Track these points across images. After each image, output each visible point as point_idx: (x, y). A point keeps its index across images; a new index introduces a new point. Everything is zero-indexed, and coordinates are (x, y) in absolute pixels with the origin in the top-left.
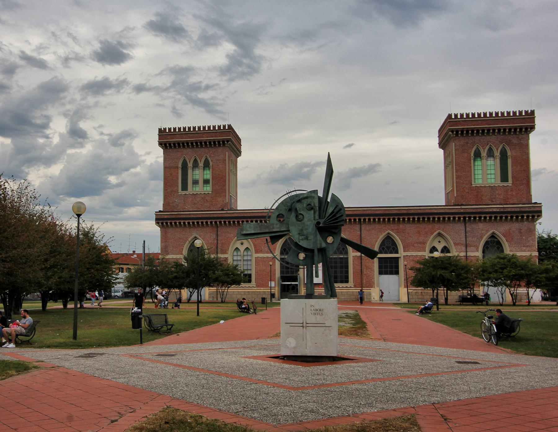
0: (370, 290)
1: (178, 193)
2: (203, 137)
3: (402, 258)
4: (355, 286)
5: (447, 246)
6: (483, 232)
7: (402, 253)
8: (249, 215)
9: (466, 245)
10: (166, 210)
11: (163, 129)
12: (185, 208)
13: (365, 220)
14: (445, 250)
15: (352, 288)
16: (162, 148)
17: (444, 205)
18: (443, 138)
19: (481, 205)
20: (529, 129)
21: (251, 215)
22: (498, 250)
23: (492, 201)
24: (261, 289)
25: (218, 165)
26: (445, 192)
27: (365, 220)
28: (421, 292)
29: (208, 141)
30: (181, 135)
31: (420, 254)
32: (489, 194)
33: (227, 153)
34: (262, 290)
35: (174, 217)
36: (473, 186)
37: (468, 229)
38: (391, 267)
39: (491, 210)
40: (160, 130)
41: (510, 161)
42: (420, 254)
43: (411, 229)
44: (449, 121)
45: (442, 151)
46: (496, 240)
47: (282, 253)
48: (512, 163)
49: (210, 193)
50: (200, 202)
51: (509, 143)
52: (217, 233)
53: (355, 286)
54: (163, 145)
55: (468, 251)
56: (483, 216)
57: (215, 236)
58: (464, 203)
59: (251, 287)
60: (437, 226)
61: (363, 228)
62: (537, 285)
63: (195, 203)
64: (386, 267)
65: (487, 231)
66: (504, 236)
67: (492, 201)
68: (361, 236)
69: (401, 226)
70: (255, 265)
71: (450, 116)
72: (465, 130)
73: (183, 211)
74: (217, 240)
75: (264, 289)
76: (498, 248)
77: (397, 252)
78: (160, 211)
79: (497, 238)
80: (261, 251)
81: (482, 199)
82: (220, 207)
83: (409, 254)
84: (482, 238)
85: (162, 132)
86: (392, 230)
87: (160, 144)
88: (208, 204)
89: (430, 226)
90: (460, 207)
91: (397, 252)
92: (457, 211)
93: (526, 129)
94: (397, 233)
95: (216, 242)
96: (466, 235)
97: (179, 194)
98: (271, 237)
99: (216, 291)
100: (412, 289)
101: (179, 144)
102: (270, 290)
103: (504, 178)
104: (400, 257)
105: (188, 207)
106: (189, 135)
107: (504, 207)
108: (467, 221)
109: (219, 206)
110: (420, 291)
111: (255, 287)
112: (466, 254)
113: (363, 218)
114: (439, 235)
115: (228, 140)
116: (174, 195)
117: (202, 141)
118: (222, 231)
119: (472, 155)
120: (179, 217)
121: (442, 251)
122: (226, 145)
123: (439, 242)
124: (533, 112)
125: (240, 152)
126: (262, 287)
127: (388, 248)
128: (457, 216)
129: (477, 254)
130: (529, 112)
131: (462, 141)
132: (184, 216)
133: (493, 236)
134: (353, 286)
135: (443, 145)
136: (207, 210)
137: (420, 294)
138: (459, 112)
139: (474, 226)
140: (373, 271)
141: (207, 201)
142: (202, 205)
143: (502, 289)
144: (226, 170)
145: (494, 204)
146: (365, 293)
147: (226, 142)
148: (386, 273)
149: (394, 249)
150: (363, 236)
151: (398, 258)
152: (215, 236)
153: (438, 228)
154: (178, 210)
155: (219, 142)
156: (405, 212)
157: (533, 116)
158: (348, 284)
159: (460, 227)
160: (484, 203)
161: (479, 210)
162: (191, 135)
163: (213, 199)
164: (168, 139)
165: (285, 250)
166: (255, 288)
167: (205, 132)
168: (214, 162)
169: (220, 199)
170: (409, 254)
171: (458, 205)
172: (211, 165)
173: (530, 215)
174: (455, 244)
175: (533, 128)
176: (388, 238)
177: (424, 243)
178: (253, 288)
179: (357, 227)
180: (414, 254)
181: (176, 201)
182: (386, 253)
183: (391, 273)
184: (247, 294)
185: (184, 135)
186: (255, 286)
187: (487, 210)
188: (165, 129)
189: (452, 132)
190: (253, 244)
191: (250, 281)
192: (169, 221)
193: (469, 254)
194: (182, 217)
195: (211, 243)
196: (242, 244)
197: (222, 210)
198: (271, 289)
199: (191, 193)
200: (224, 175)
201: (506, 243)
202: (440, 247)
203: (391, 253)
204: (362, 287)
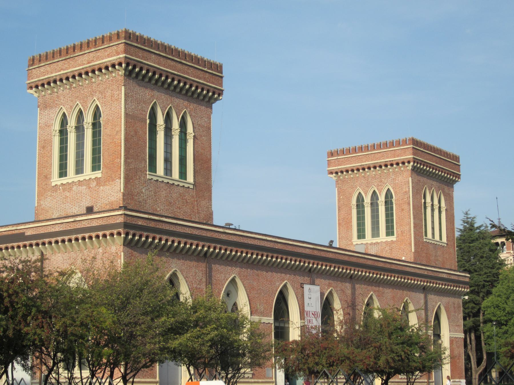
2: (188, 74)
12: (156, 210)
23: (436, 264)
35: (152, 225)
73: (166, 217)
97: (148, 177)
109: (202, 216)
115: (221, 92)
120: (160, 226)
141: (187, 202)
142: (180, 209)
162: (173, 63)
164: (139, 57)
169: (203, 203)
181: (144, 191)
185: (162, 59)
186: (251, 376)
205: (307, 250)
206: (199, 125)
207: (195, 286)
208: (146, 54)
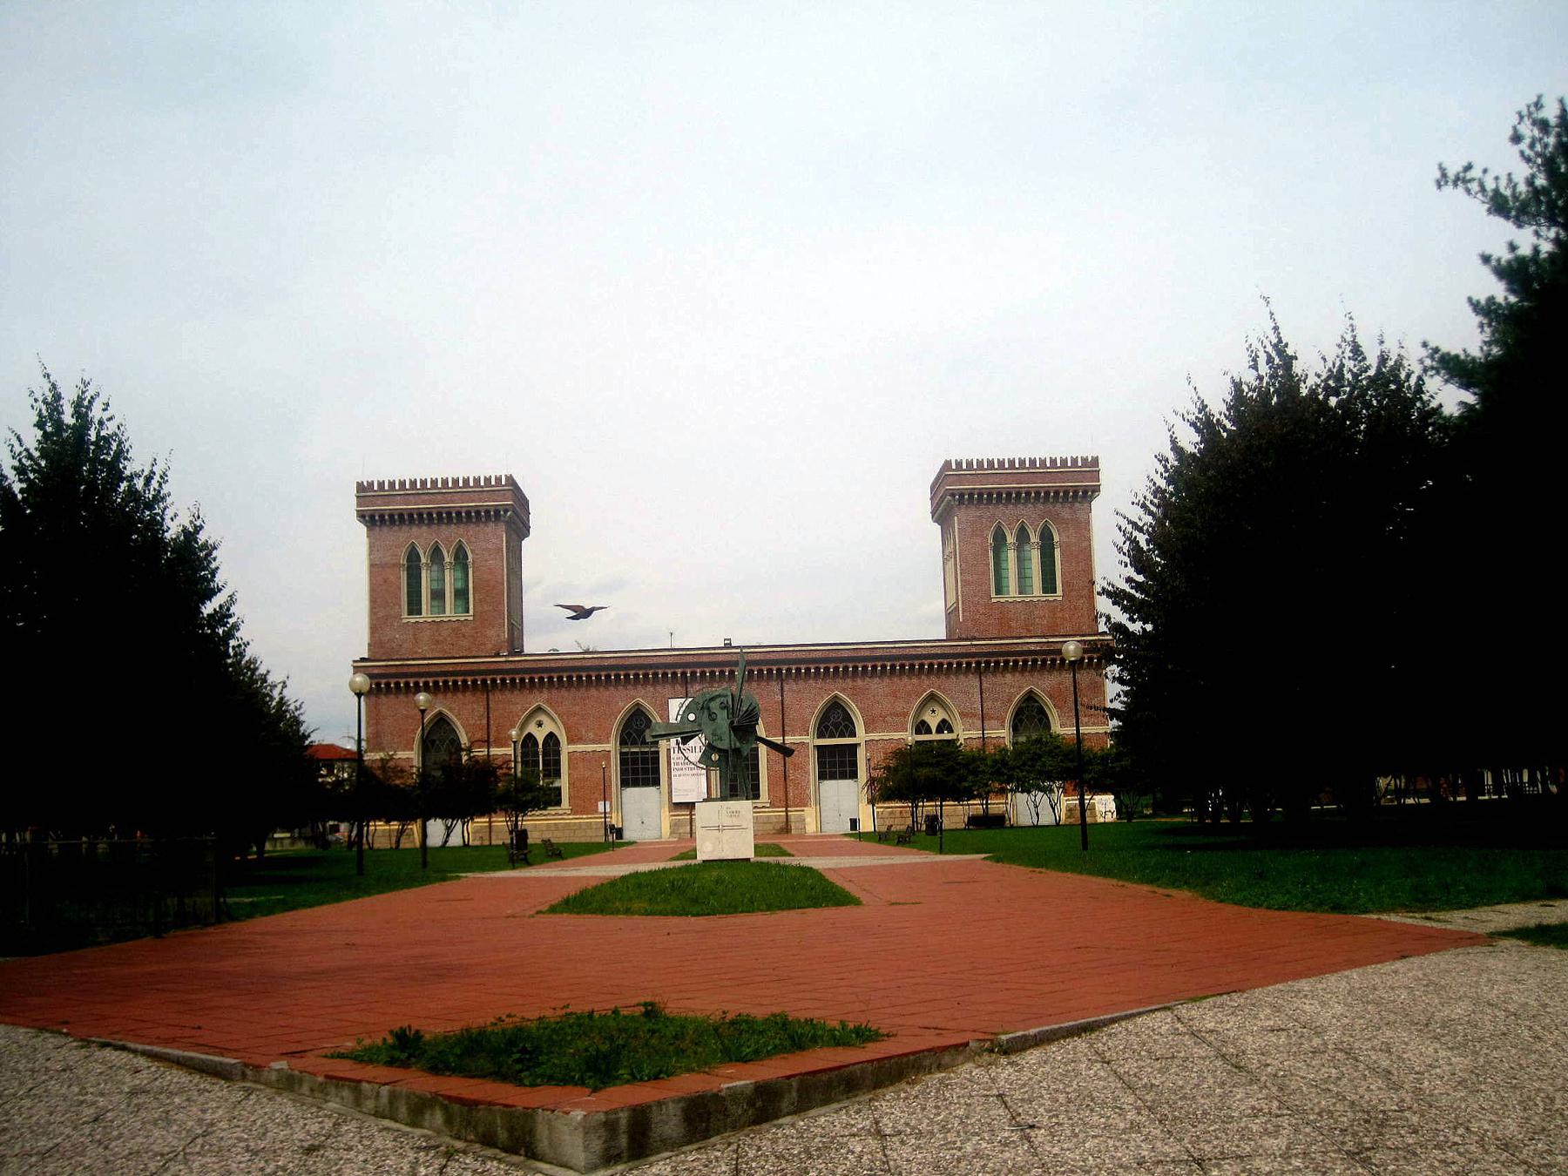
0: (803, 811)
1: (401, 619)
3: (863, 744)
4: (772, 805)
5: (947, 718)
6: (1012, 690)
7: (861, 735)
8: (553, 665)
9: (982, 715)
10: (378, 657)
11: (365, 484)
12: (416, 652)
13: (789, 670)
14: (944, 726)
15: (767, 810)
16: (365, 523)
17: (945, 638)
18: (938, 505)
19: (1007, 638)
20: (1090, 493)
21: (559, 664)
22: (1041, 723)
23: (1029, 631)
24: (582, 818)
25: (486, 561)
26: (946, 611)
27: (789, 670)
28: (901, 812)
29: (464, 510)
30: (406, 497)
31: (896, 735)
32: (1023, 617)
33: (504, 536)
34: (584, 819)
35: (393, 670)
36: (993, 600)
37: (985, 685)
38: (842, 764)
39: (1025, 648)
40: (360, 487)
41: (1057, 553)
42: (896, 735)
43: (878, 687)
44: (946, 475)
45: (937, 528)
46: (1036, 704)
47: (623, 743)
48: (1062, 554)
49: (471, 618)
50: (449, 639)
51: (1057, 519)
52: (488, 705)
53: (772, 805)
54: (367, 518)
55: (985, 728)
56: (1012, 659)
57: (482, 709)
58: (976, 635)
59: (561, 815)
60: (925, 681)
61: (786, 688)
62: (1104, 791)
63: (438, 641)
64: (833, 765)
65: (1020, 688)
66: (1051, 697)
67: (1029, 631)
68: (782, 704)
69: (859, 682)
70: (569, 768)
71: (947, 464)
72: (976, 491)
73: (414, 659)
74: (488, 717)
75: (588, 818)
76: (1040, 720)
77: (853, 734)
78: (363, 660)
79: (1037, 702)
80: (581, 739)
81: (1010, 627)
82: (492, 649)
83: (875, 736)
84: (1010, 701)
85: (363, 490)
86: (843, 690)
87: (362, 516)
88: (465, 643)
89: (915, 681)
90: (969, 643)
91: (853, 734)
92: (964, 650)
93: (1085, 492)
94: (853, 696)
95: (485, 722)
96: (982, 697)
98: (682, 738)
99: (487, 824)
100: (881, 807)
101: (401, 515)
102: (603, 820)
103: (1049, 586)
104: (860, 744)
105: (424, 649)
106: (423, 496)
107: (1048, 642)
108: (982, 670)
109: (489, 646)
110: (899, 809)
111: (569, 814)
112: (983, 734)
113: (787, 667)
114: (932, 698)
115: (507, 507)
116: (392, 625)
117: (451, 510)
118: (496, 697)
119: (991, 541)
120: (405, 670)
121: (940, 730)
122: (502, 519)
123: (933, 711)
124: (1095, 461)
125: (528, 528)
126: (582, 813)
127: (836, 726)
128: (964, 660)
129: (1002, 734)
130: (1090, 459)
131: (972, 513)
132: (416, 670)
133: (1030, 698)
134: (768, 805)
135: (942, 515)
136: (465, 654)
137: (898, 815)
138: (964, 457)
139: (999, 679)
140: (807, 773)
141: (464, 636)
143: (1035, 796)
144: (503, 570)
145: (1031, 637)
146: (792, 817)
147: (502, 513)
148: (833, 777)
149: (846, 727)
150: (786, 703)
151: (854, 747)
152: (482, 710)
153: (930, 685)
154: (402, 657)
155: (487, 512)
156: (867, 653)
157: (1094, 469)
158: (757, 801)
159: (972, 682)
160: (1014, 635)
161: (1004, 649)
162: (426, 497)
163: (477, 633)
165: (629, 735)
166: (571, 817)
167: (459, 490)
168: (477, 554)
169: (491, 633)
170: (875, 736)
171: (966, 640)
172: (470, 559)
173: (1095, 656)
174: (962, 715)
175: (1096, 489)
176: (835, 707)
177: (905, 715)
178: (565, 817)
179: (775, 686)
180: (886, 736)
181: (397, 636)
182: (832, 736)
183: (843, 776)
184: (553, 829)
185: (411, 498)
187: (1019, 649)
188: (371, 484)
189: (953, 495)
190: (564, 725)
191: (558, 803)
192: (383, 681)
193: (991, 733)
194: (412, 670)
195: (474, 724)
196: (540, 724)
197: (497, 655)
198: (605, 818)
199: (430, 620)
200: (500, 581)
201: (1054, 711)
202: (933, 721)
203: (842, 735)
204: (787, 806)
205: (669, 658)
206: (484, 550)
207: (472, 722)
208: (386, 499)
